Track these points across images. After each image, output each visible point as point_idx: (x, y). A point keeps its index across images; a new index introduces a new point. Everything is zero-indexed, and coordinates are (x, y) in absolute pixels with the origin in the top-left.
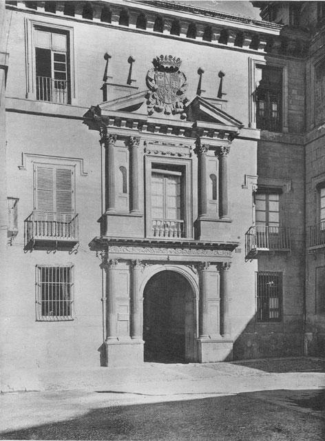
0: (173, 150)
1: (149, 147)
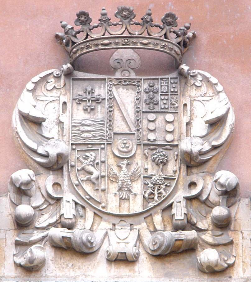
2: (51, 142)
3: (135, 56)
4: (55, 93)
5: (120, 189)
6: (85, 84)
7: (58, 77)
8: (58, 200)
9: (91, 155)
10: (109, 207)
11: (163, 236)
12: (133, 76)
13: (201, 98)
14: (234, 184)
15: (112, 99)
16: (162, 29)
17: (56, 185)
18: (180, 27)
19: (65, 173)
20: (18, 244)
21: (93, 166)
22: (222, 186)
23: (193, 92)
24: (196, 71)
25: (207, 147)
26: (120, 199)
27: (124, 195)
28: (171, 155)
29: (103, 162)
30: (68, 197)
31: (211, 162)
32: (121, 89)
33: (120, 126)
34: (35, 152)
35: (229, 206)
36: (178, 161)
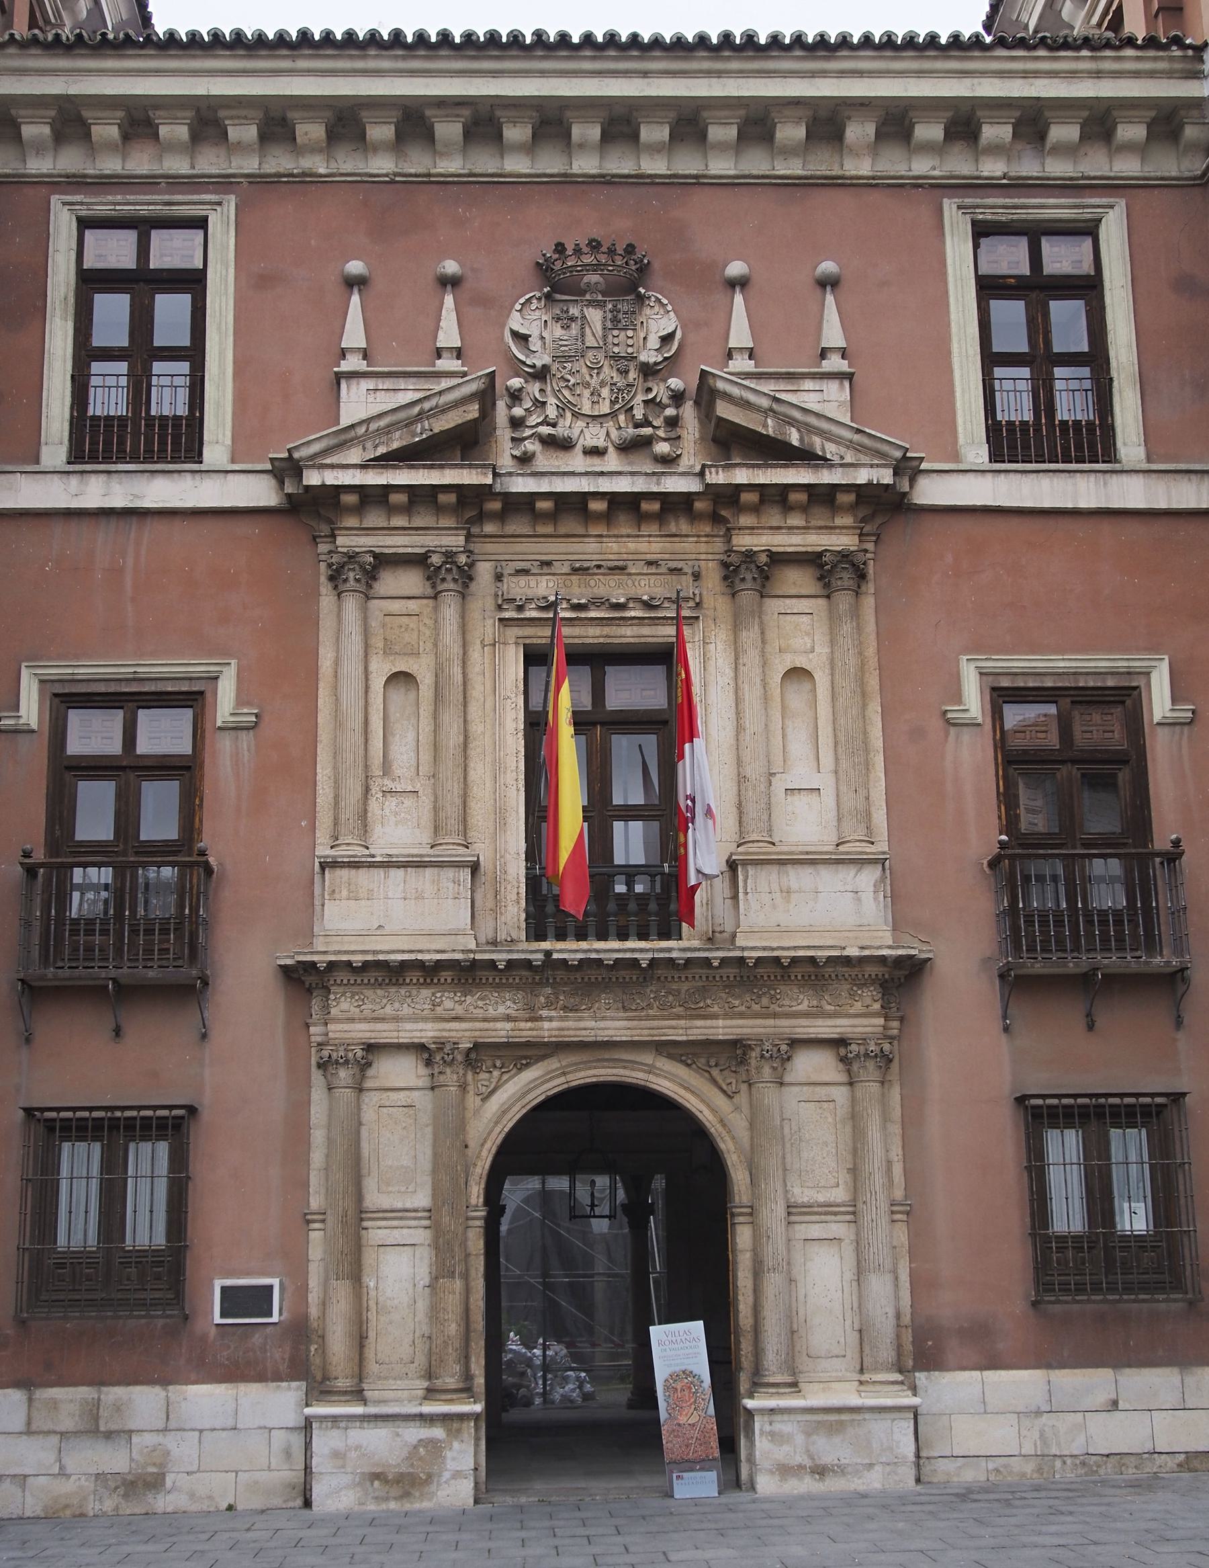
1: (518, 588)
4: (537, 313)
5: (592, 394)
6: (561, 305)
7: (539, 299)
8: (544, 403)
9: (568, 365)
12: (600, 298)
17: (541, 390)
19: (548, 381)
20: (513, 439)
22: (672, 390)
23: (647, 311)
24: (650, 293)
25: (660, 359)
27: (595, 399)
29: (578, 371)
30: (552, 401)
31: (664, 371)
33: (590, 341)
34: (524, 363)
35: (678, 406)
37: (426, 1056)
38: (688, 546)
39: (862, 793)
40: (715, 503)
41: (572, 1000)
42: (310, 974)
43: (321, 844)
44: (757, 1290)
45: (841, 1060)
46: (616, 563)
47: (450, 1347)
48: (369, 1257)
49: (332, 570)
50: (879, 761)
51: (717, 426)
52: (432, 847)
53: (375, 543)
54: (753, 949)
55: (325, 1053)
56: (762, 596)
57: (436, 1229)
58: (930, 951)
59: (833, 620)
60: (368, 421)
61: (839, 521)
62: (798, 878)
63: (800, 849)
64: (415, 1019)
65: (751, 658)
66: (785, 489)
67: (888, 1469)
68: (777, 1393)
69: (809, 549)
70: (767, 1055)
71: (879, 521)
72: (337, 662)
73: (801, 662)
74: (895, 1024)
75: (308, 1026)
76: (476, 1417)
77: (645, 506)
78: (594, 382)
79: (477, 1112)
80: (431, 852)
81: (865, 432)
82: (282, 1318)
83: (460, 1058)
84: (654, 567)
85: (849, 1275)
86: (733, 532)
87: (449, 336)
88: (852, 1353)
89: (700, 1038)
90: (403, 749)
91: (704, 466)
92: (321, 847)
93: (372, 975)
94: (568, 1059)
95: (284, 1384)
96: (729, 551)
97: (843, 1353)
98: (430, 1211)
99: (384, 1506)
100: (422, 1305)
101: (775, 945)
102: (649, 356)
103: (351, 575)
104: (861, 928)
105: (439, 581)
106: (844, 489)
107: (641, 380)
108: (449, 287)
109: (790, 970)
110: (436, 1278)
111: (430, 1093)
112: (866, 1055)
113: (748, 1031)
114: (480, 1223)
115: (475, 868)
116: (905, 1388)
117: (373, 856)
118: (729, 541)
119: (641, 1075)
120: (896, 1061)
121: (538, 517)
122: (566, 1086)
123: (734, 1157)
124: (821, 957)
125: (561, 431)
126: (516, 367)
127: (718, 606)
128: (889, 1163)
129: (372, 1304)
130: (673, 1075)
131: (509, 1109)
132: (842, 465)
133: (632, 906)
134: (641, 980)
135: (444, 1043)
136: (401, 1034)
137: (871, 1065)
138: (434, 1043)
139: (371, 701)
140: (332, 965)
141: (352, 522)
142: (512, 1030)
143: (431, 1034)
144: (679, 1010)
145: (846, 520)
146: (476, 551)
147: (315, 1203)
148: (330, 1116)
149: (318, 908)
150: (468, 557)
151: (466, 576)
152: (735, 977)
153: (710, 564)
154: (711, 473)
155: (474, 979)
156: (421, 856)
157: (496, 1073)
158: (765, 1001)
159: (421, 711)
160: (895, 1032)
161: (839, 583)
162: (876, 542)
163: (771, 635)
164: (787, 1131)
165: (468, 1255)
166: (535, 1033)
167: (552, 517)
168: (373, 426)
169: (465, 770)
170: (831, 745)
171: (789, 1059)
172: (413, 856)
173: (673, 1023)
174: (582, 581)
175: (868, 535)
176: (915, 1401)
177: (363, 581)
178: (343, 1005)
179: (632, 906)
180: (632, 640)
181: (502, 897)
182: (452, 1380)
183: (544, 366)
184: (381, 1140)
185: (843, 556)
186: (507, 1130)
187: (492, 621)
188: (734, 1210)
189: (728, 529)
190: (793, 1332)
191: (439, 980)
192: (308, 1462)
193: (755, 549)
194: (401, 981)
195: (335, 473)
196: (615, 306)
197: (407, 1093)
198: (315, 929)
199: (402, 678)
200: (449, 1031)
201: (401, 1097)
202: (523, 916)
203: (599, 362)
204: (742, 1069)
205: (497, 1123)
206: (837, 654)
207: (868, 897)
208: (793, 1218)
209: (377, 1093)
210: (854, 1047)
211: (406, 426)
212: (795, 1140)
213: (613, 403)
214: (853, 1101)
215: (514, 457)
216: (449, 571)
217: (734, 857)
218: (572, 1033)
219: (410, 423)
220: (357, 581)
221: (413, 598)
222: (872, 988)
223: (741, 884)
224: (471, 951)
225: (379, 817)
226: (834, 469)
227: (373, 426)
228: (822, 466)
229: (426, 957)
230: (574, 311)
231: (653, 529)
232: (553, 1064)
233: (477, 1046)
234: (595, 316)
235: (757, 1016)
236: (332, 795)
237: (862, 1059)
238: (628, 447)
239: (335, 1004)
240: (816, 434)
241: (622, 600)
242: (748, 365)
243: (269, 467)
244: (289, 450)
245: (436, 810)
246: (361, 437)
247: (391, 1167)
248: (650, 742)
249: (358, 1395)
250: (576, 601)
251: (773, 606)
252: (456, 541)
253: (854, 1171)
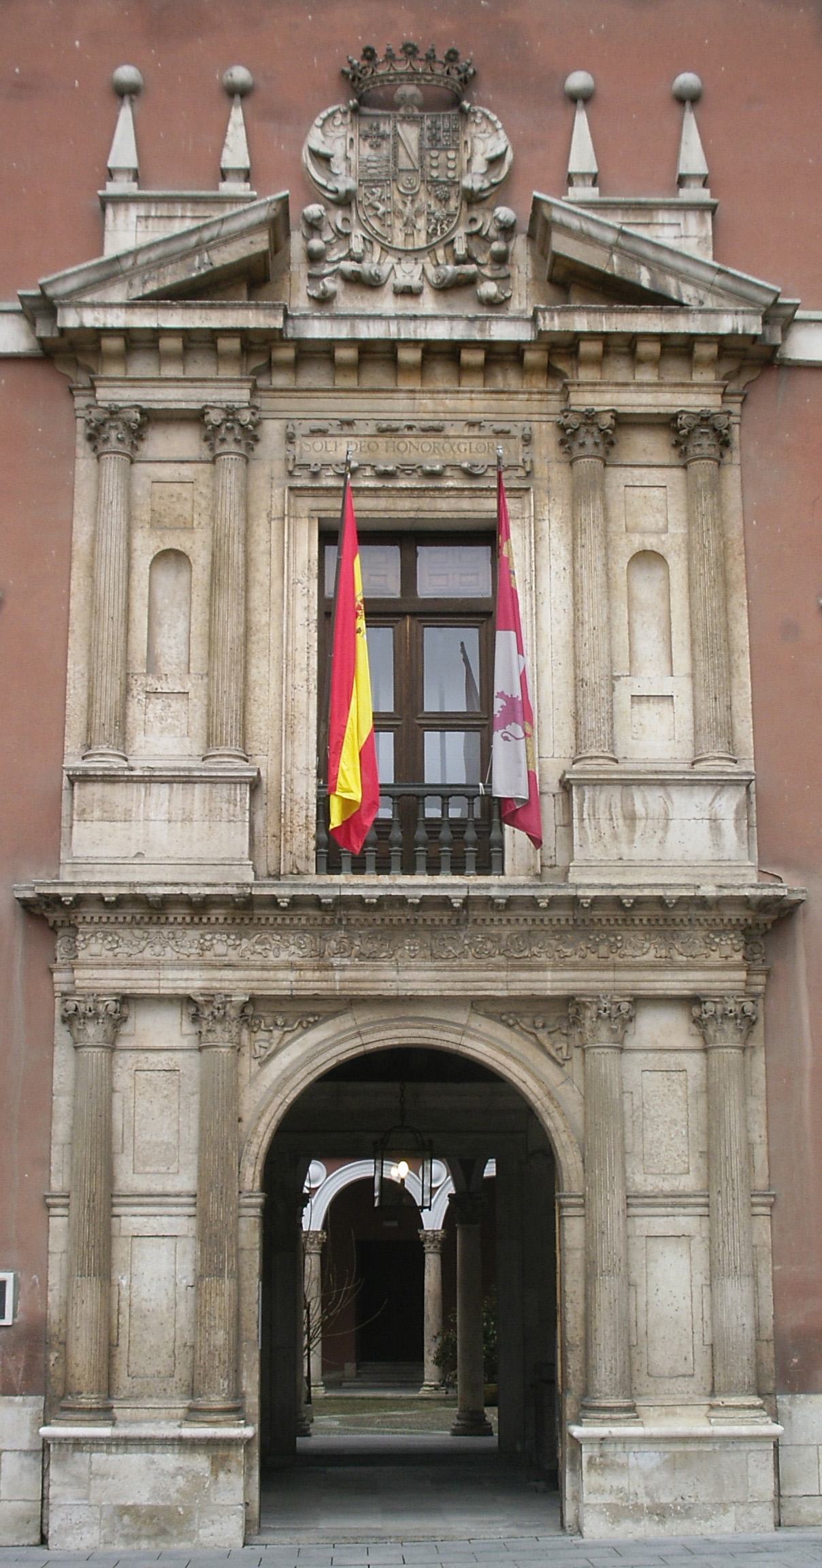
0: (429, 453)
1: (314, 450)
2: (341, 178)
3: (418, 92)
4: (342, 130)
5: (405, 225)
6: (370, 120)
7: (345, 114)
8: (348, 235)
9: (378, 191)
10: (395, 242)
11: (446, 270)
12: (416, 112)
13: (480, 135)
14: (512, 221)
15: (396, 135)
16: (445, 66)
17: (345, 220)
18: (462, 64)
19: (354, 209)
20: (310, 277)
21: (379, 201)
22: (500, 222)
23: (472, 129)
24: (476, 108)
25: (486, 185)
26: (406, 234)
28: (453, 191)
29: (389, 198)
31: (490, 199)
32: (405, 126)
34: (325, 188)
36: (460, 198)
37: (192, 1010)
38: (517, 404)
39: (723, 701)
40: (550, 355)
41: (369, 946)
42: (54, 910)
43: (70, 754)
44: (588, 1298)
45: (694, 1022)
46: (431, 424)
47: (217, 1358)
48: (121, 1251)
49: (91, 428)
50: (744, 664)
51: (554, 264)
52: (203, 760)
53: (142, 397)
54: (589, 886)
55: (71, 1005)
56: (605, 465)
57: (203, 1218)
58: (803, 891)
59: (692, 493)
60: (135, 253)
61: (698, 377)
62: (646, 802)
63: (650, 767)
64: (179, 965)
65: (591, 539)
66: (632, 340)
67: (742, 1509)
68: (612, 1419)
69: (662, 410)
70: (604, 1014)
71: (746, 377)
72: (95, 538)
73: (651, 543)
74: (761, 979)
75: (51, 972)
76: (248, 1442)
77: (467, 357)
78: (408, 210)
79: (253, 1079)
80: (202, 765)
81: (727, 273)
82: (16, 1320)
83: (233, 1013)
84: (476, 429)
85: (700, 1279)
86: (570, 388)
87: (236, 154)
88: (702, 1371)
89: (524, 993)
90: (172, 642)
91: (536, 310)
92: (71, 758)
93: (128, 912)
94: (364, 1016)
95: (18, 1399)
96: (566, 411)
97: (691, 1372)
98: (195, 1196)
99: (135, 1546)
100: (185, 1309)
101: (615, 882)
102: (474, 181)
103: (113, 434)
104: (719, 864)
105: (218, 442)
106: (704, 339)
107: (464, 209)
108: (237, 99)
109: (634, 913)
110: (201, 1276)
111: (196, 1055)
112: (724, 1016)
113: (583, 985)
114: (257, 1212)
115: (255, 785)
116: (764, 1413)
117: (132, 769)
118: (567, 399)
119: (452, 1037)
120: (761, 1022)
121: (337, 367)
122: (361, 1049)
123: (564, 1137)
124: (671, 898)
125: (367, 267)
126: (314, 192)
127: (553, 475)
128: (750, 1145)
129: (124, 1304)
130: (491, 1037)
131: (292, 1075)
132: (701, 311)
133: (445, 834)
134: (453, 922)
135: (213, 996)
136: (162, 983)
137: (729, 1027)
138: (202, 995)
139: (134, 583)
140: (79, 900)
141: (115, 371)
142: (297, 981)
143: (198, 984)
144: (499, 959)
145: (706, 376)
146: (263, 407)
147: (58, 1183)
148: (76, 1081)
149: (65, 831)
150: (253, 414)
151: (250, 437)
152: (567, 920)
153: (544, 426)
154: (544, 318)
155: (251, 919)
156: (190, 769)
157: (277, 1033)
158: (603, 950)
159: (194, 597)
160: (760, 988)
161: (698, 450)
162: (742, 403)
163: (616, 511)
164: (627, 1106)
165: (240, 1250)
166: (324, 985)
167: (357, 367)
168: (142, 259)
169: (246, 668)
170: (687, 644)
171: (631, 1020)
172: (179, 769)
173: (492, 975)
174: (390, 444)
175: (733, 395)
176: (777, 1429)
177: (127, 442)
178: (93, 947)
179: (445, 834)
180: (449, 515)
181: (288, 820)
182: (218, 1398)
183: (348, 192)
184: (138, 1110)
185: (702, 419)
186: (289, 1101)
187: (281, 489)
188: (562, 1200)
189: (565, 386)
190: (630, 1347)
191: (209, 919)
192: (45, 1492)
193: (597, 409)
194: (163, 920)
195: (96, 314)
196: (434, 123)
197: (170, 1054)
198: (62, 856)
199: (172, 556)
200: (221, 980)
201: (162, 1060)
202: (313, 844)
203: (415, 188)
204: (575, 1032)
205: (277, 1092)
206: (694, 535)
207: (728, 826)
208: (633, 1211)
209: (134, 1055)
210: (709, 1006)
211: (182, 259)
212: (638, 1117)
213: (430, 235)
214: (707, 1071)
215: (311, 297)
216: (230, 430)
217: (567, 776)
218: (368, 985)
219: (187, 254)
220: (120, 440)
221: (188, 462)
222: (732, 936)
223: (575, 808)
224: (248, 885)
225: (142, 723)
226: (691, 316)
227: (142, 259)
228: (678, 312)
229: (193, 891)
230: (386, 128)
231: (474, 383)
232: (345, 1022)
233: (253, 1000)
234: (410, 134)
235: (593, 967)
236: (85, 696)
237: (720, 1020)
238: (447, 288)
239: (83, 945)
240: (671, 275)
241: (438, 468)
242: (590, 193)
243: (18, 306)
244: (42, 287)
245: (209, 715)
246: (127, 271)
247: (149, 1143)
248: (470, 636)
249: (105, 1413)
250: (382, 468)
251: (618, 477)
252: (239, 395)
253: (709, 1155)
